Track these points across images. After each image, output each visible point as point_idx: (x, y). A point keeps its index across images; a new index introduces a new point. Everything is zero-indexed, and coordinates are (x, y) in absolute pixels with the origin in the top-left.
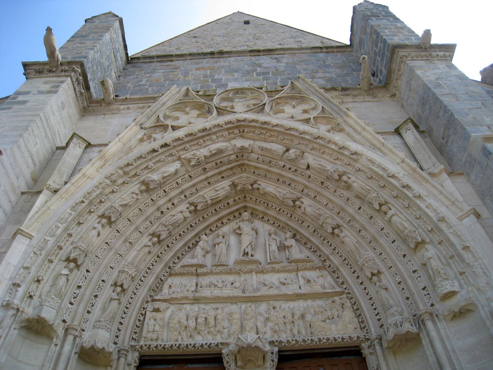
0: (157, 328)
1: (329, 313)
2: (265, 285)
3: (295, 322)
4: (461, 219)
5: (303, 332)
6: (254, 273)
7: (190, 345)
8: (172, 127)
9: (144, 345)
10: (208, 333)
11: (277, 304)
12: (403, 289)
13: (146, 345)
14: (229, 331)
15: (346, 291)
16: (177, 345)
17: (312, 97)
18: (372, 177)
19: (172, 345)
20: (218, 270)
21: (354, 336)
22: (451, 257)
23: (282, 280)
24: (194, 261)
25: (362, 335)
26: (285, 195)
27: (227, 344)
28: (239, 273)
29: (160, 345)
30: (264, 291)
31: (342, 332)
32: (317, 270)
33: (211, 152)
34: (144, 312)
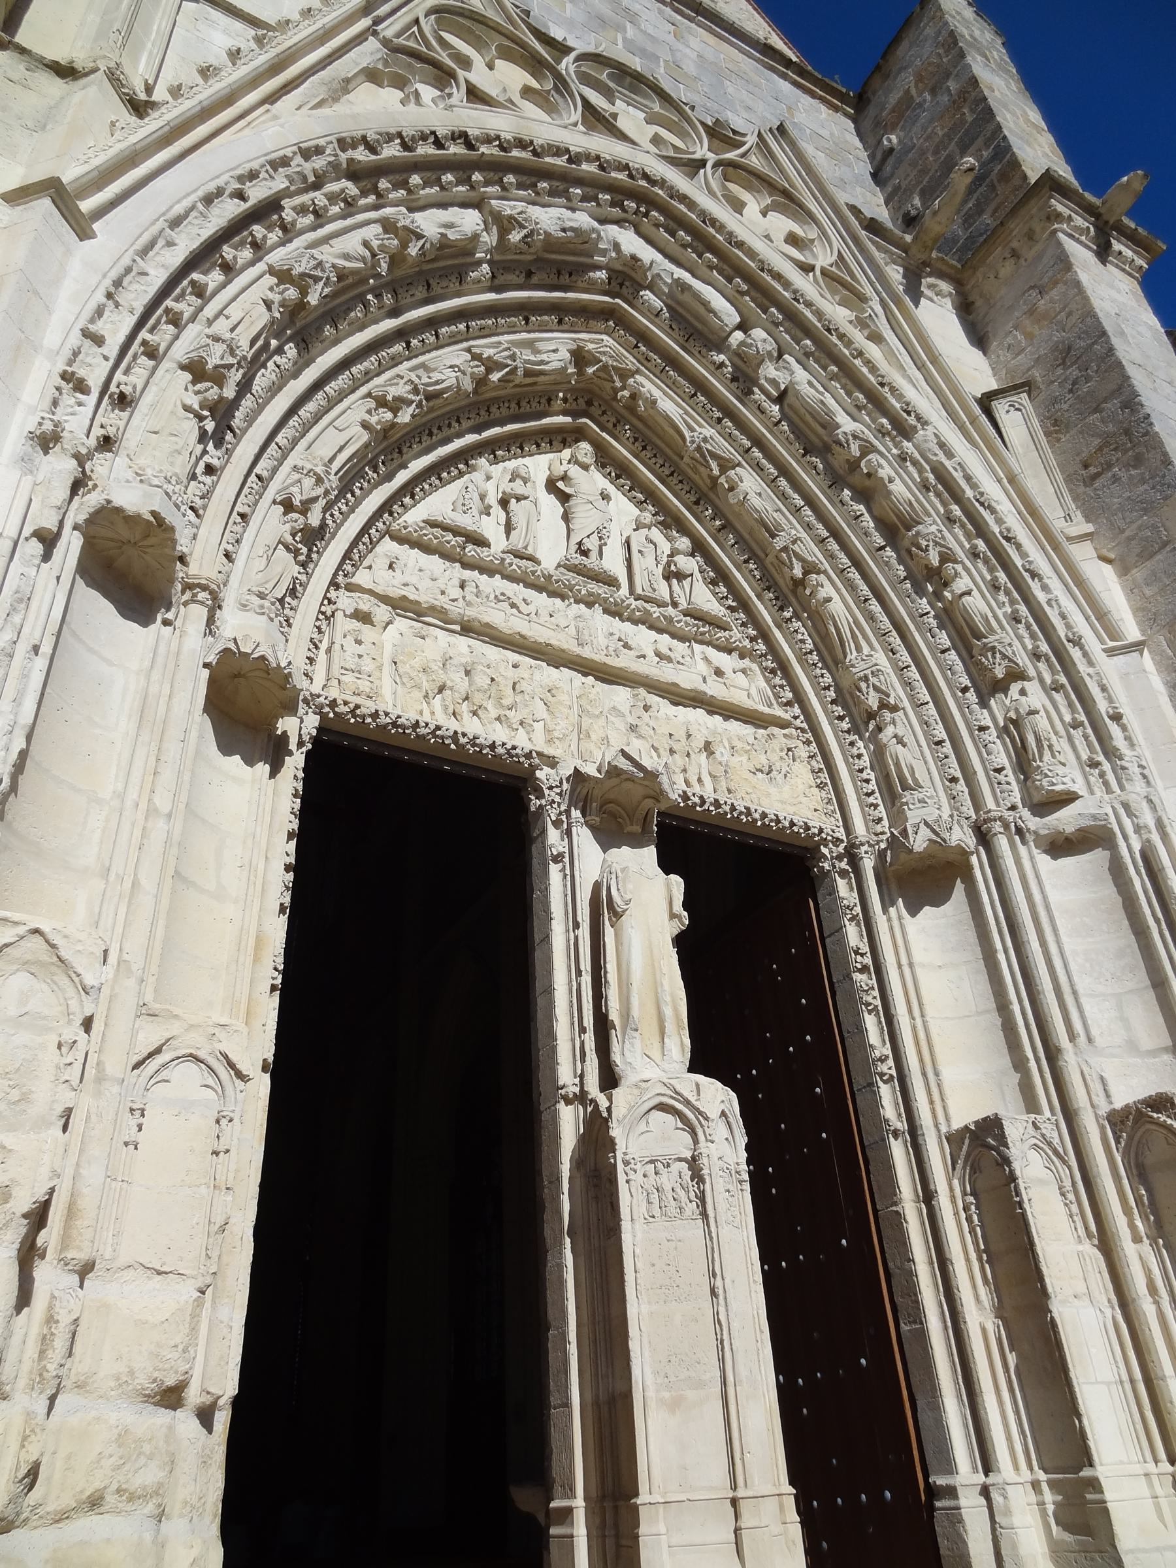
0: (368, 665)
2: (626, 646)
3: (693, 756)
4: (1111, 652)
5: (707, 779)
6: (598, 609)
7: (464, 735)
9: (339, 702)
10: (498, 719)
11: (653, 699)
12: (946, 757)
13: (346, 703)
14: (548, 731)
15: (798, 723)
16: (432, 727)
19: (417, 721)
20: (519, 567)
21: (815, 824)
23: (664, 650)
24: (465, 521)
25: (831, 825)
26: (705, 440)
27: (552, 762)
28: (563, 597)
29: (387, 714)
30: (624, 661)
31: (792, 809)
32: (735, 655)
33: (564, 230)
34: (329, 613)
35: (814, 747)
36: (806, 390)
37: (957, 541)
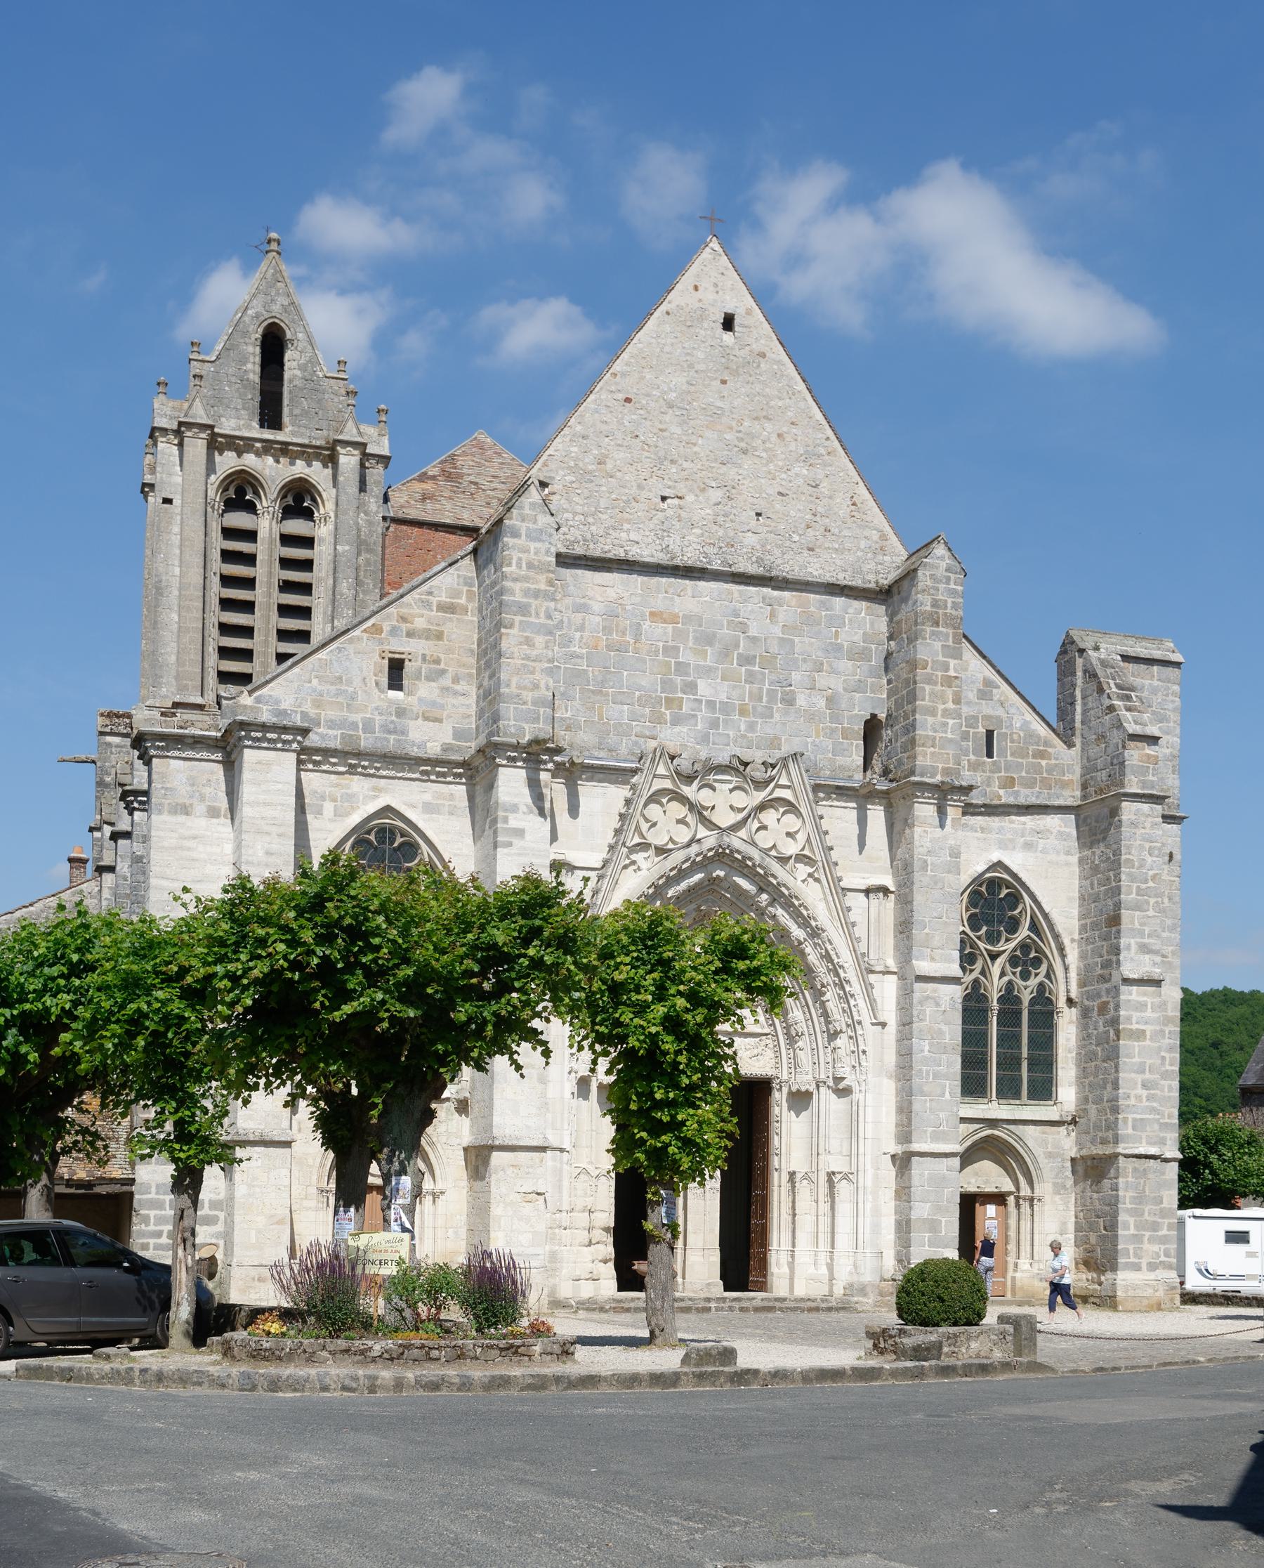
1: (756, 1052)
4: (873, 1024)
8: (656, 848)
17: (802, 810)
18: (827, 957)
22: (853, 1052)
35: (776, 1043)
36: (781, 919)
37: (829, 979)
